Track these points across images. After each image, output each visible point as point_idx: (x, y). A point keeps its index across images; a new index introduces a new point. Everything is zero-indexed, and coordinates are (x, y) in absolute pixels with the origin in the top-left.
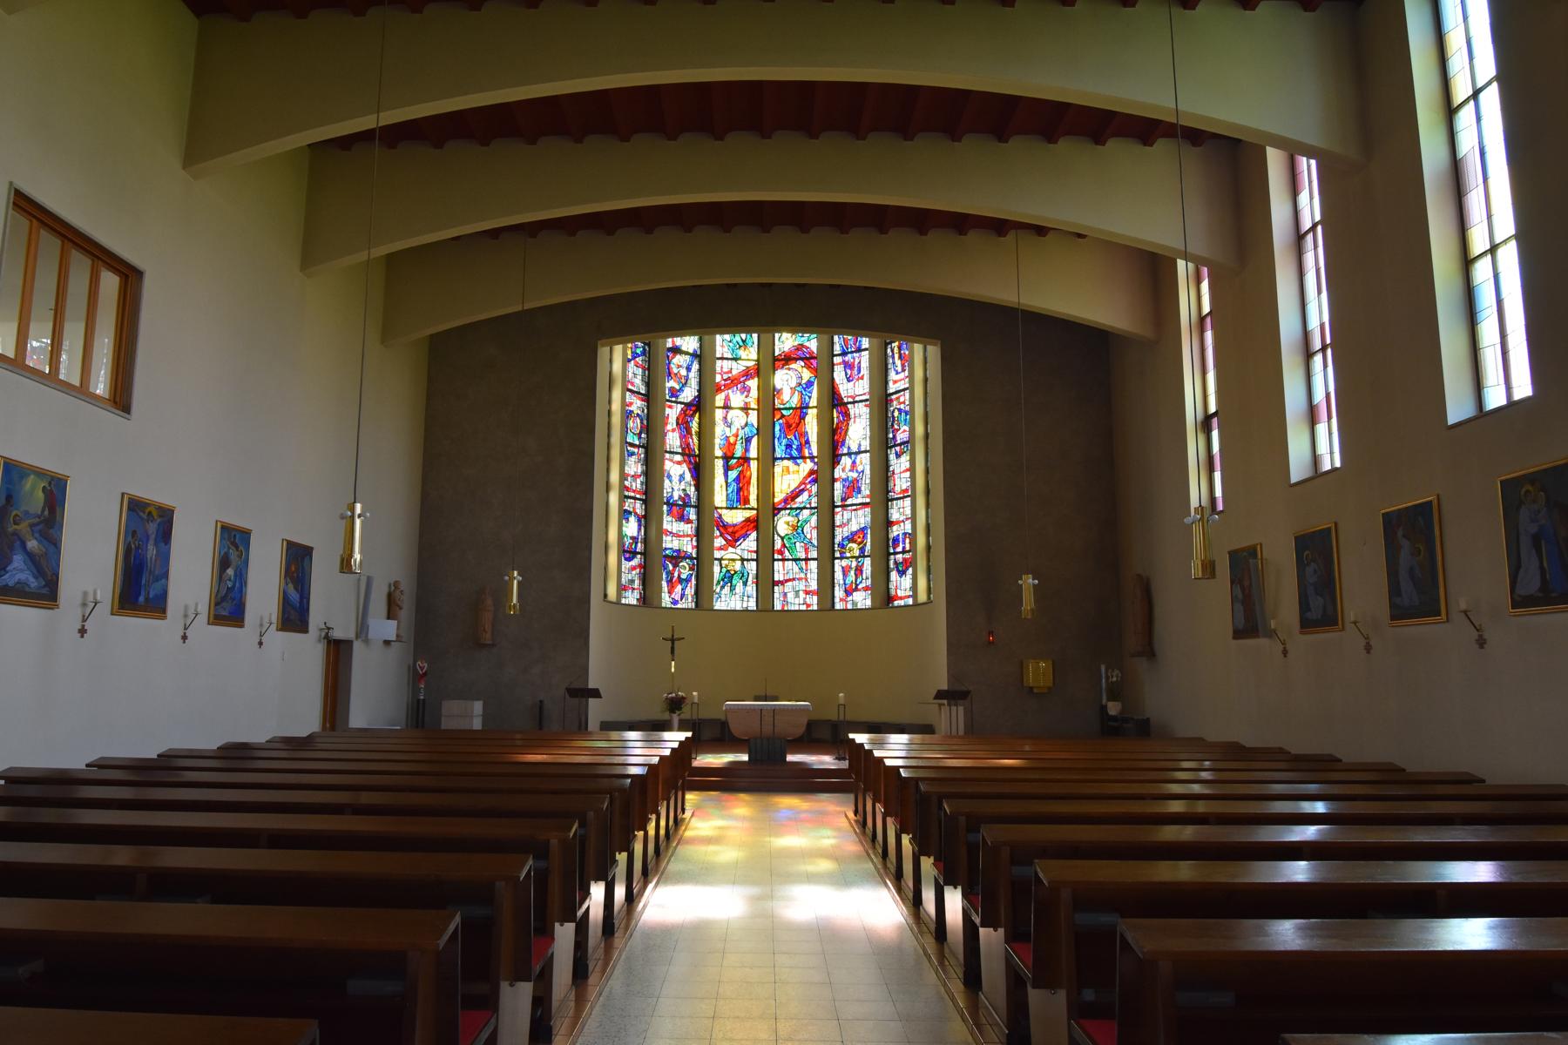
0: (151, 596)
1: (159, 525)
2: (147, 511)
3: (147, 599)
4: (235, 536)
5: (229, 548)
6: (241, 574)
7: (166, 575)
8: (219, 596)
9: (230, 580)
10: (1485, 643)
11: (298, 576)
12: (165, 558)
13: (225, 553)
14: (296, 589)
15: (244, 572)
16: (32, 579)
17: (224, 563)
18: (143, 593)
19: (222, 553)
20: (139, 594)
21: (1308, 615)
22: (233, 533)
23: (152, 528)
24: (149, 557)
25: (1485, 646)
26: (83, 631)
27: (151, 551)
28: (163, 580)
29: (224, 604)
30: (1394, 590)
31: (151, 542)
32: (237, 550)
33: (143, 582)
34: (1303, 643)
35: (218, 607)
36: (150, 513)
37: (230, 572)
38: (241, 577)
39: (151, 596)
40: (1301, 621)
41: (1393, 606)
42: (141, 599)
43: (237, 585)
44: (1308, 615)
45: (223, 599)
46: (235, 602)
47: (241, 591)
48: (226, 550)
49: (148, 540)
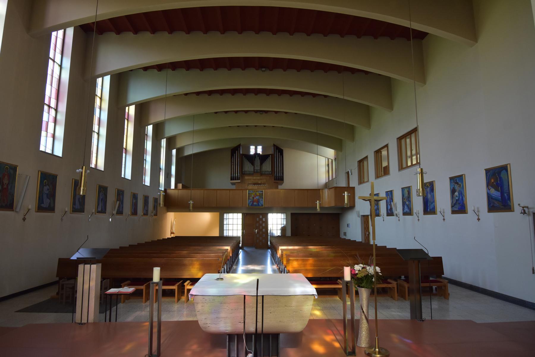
0: (431, 208)
1: (430, 188)
2: (426, 186)
3: (430, 210)
4: (456, 180)
5: (454, 185)
6: (461, 193)
7: (434, 202)
8: (453, 204)
9: (457, 197)
10: (26, 219)
11: (497, 184)
12: (433, 197)
13: (453, 187)
14: (497, 190)
15: (462, 192)
16: (408, 210)
17: (453, 191)
18: (429, 208)
19: (452, 188)
20: (428, 209)
21: (42, 205)
22: (455, 179)
23: (428, 189)
24: (429, 198)
25: (25, 220)
26: (419, 220)
27: (429, 196)
28: (433, 203)
29: (456, 206)
30: (74, 203)
31: (429, 193)
32: (458, 185)
33: (428, 205)
34: (35, 216)
35: (453, 208)
36: (427, 186)
37: (456, 194)
38: (462, 194)
39: (431, 208)
40: (38, 207)
41: (73, 208)
42: (429, 210)
43: (460, 197)
44: (42, 205)
45: (455, 204)
46: (460, 204)
47: (462, 199)
48: (453, 186)
49: (428, 193)
